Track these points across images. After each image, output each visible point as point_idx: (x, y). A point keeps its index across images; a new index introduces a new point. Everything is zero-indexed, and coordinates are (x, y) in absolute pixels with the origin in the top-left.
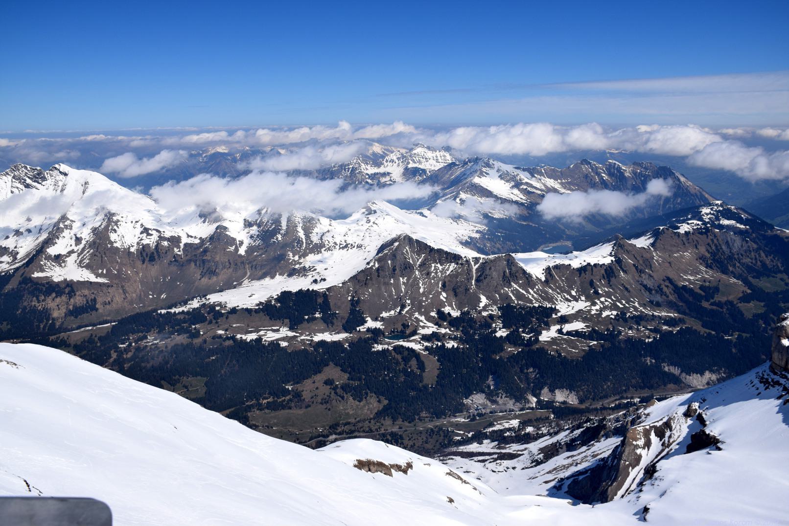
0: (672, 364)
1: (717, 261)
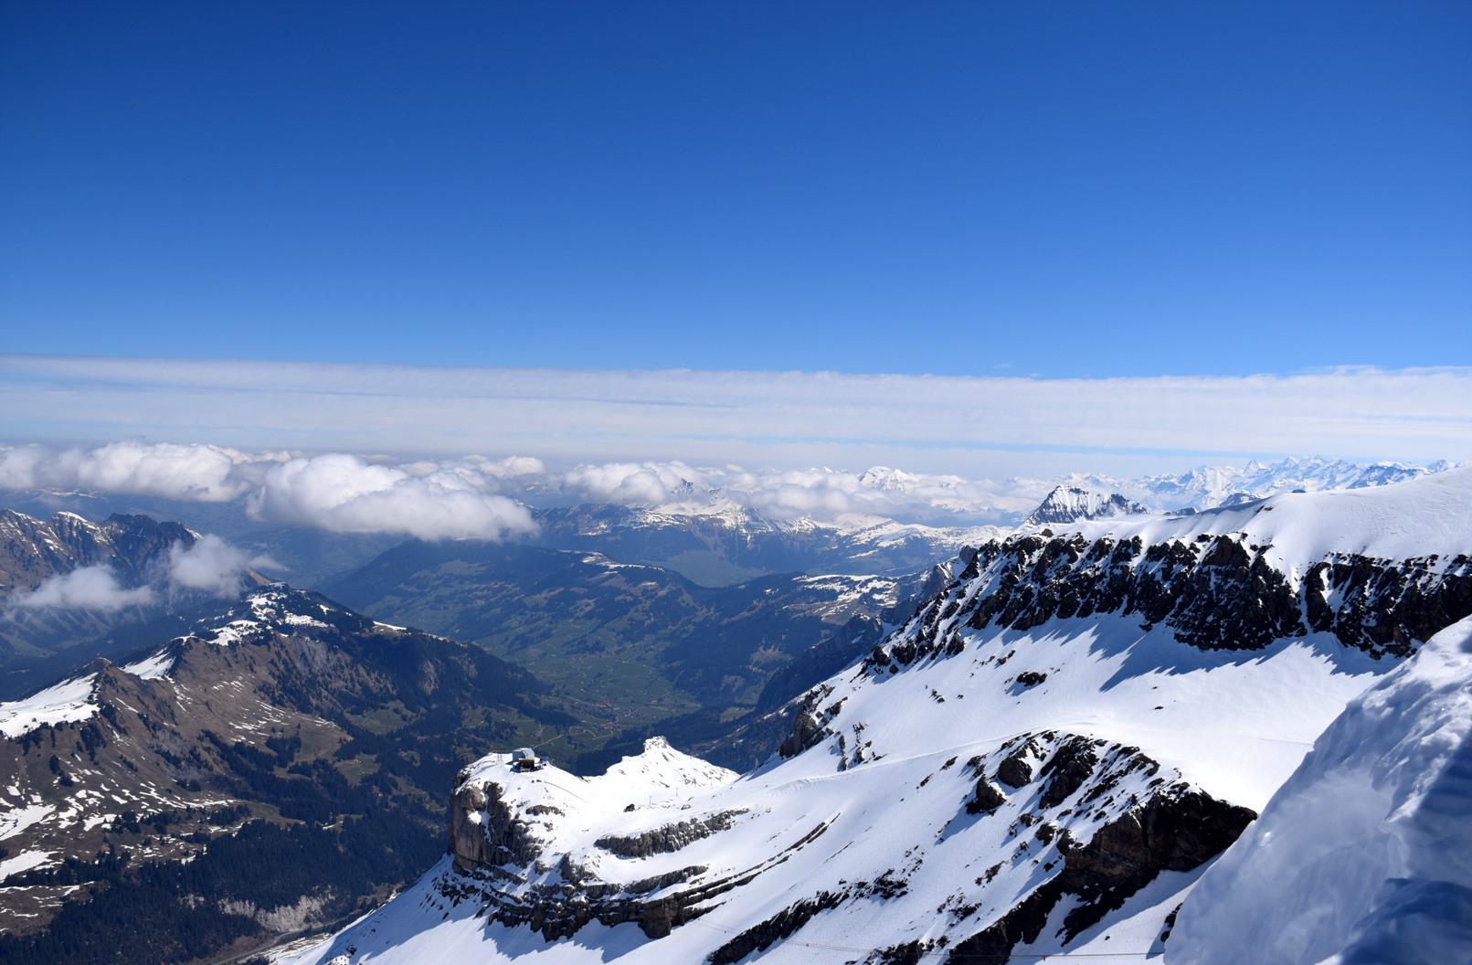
0: (237, 898)
1: (291, 692)
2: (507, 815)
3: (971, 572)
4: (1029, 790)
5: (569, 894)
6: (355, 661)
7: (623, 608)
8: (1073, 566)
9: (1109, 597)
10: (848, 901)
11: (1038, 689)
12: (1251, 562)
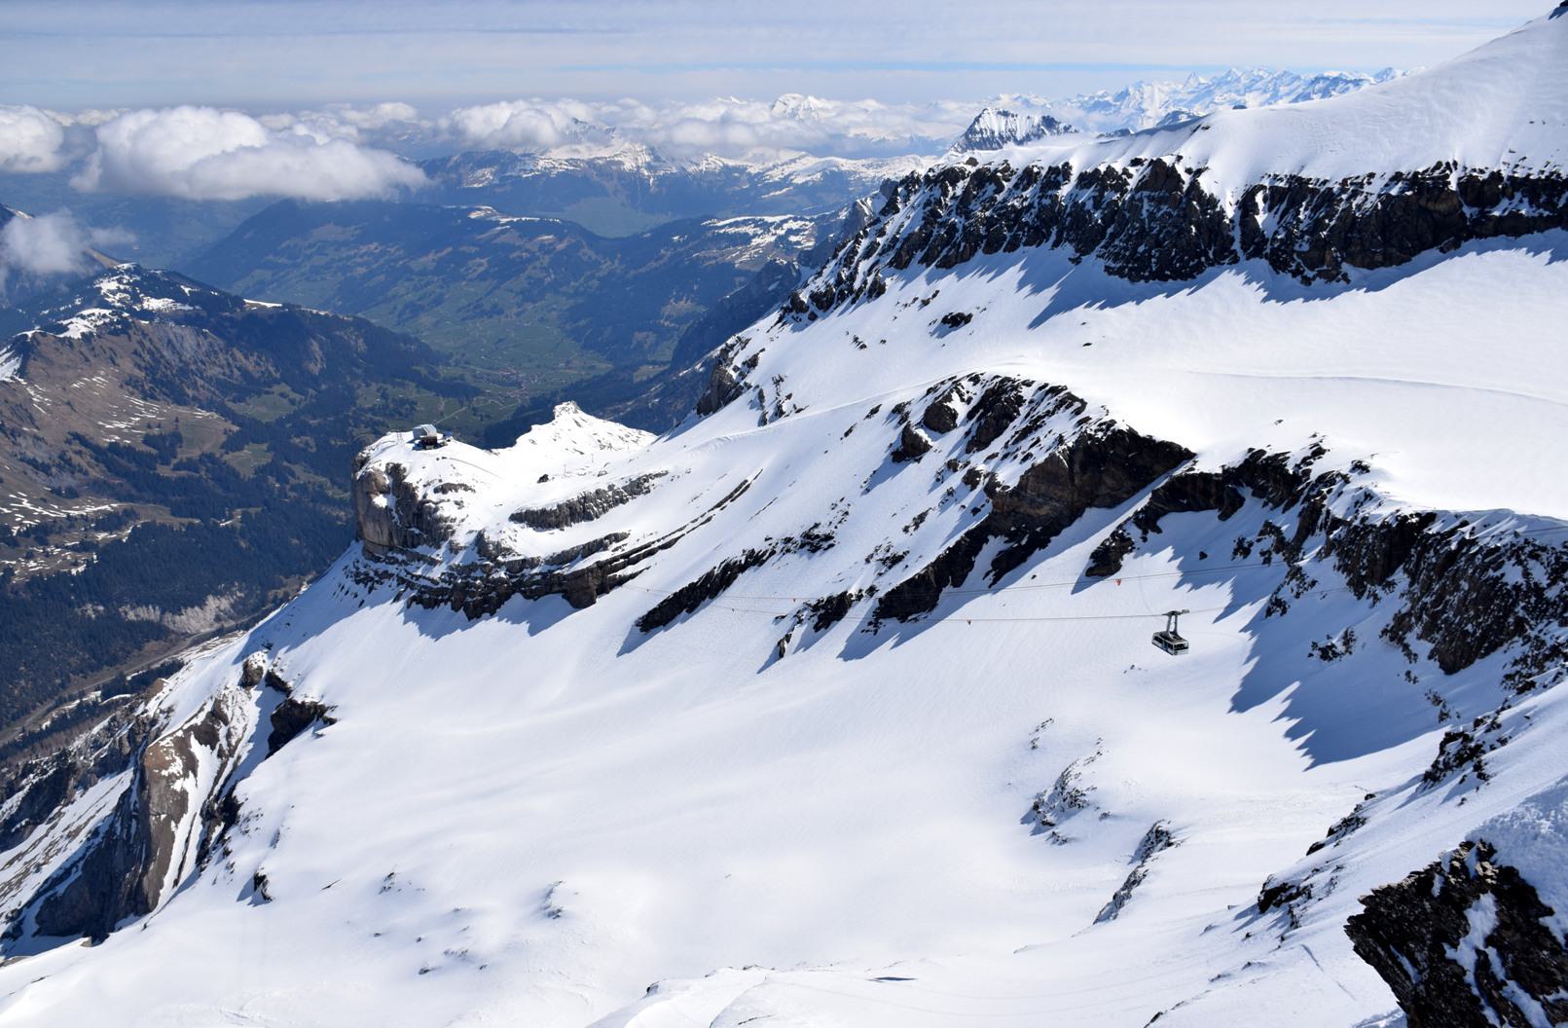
0: (139, 603)
2: (414, 496)
3: (891, 208)
4: (956, 435)
5: (488, 571)
6: (230, 344)
7: (521, 265)
8: (999, 197)
9: (1037, 229)
10: (775, 558)
11: (964, 330)
12: (1185, 187)
